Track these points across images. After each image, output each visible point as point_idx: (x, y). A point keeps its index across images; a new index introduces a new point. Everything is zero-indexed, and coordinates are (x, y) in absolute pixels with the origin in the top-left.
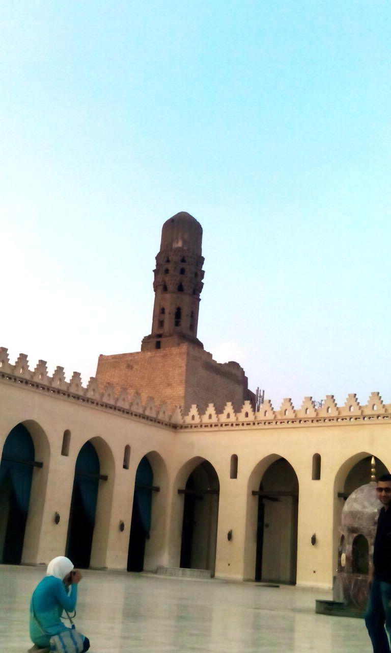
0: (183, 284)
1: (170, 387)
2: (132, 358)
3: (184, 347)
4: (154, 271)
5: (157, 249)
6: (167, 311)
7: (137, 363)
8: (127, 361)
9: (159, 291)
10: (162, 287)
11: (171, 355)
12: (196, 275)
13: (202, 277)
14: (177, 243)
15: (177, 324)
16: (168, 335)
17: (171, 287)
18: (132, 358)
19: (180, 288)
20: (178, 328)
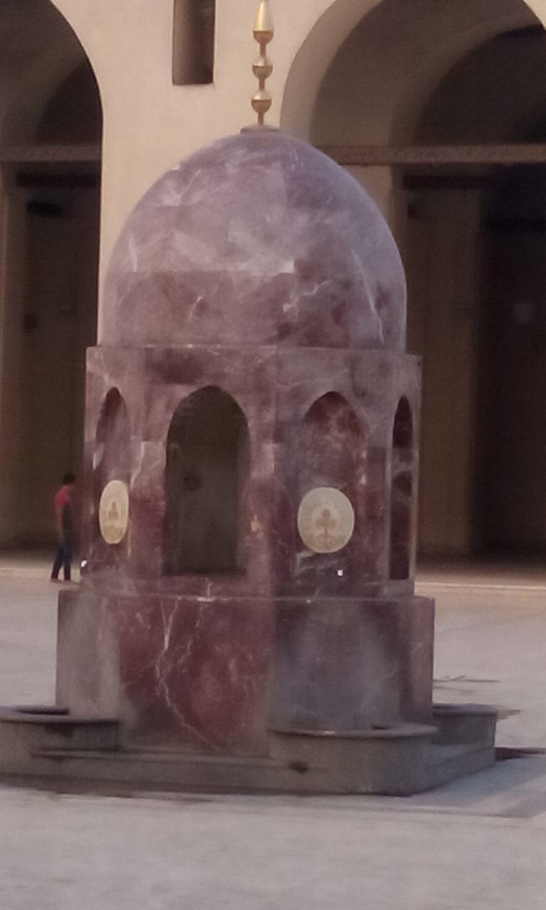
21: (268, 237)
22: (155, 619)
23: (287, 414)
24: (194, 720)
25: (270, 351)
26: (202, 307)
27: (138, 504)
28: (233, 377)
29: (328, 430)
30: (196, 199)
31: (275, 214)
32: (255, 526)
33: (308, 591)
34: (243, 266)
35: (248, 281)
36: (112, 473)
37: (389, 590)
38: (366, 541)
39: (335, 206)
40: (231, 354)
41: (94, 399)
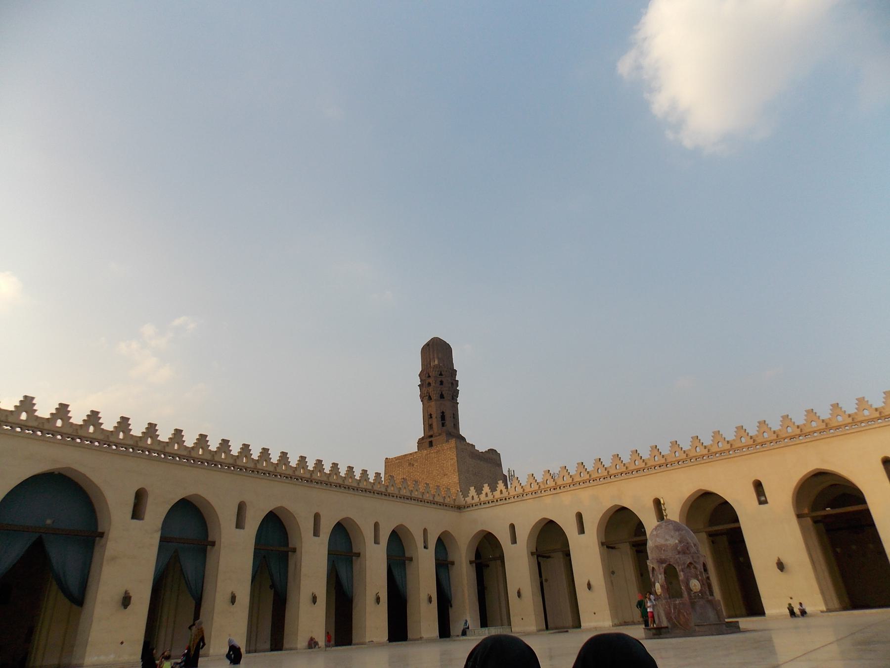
0: (443, 393)
1: (446, 476)
2: (412, 457)
3: (453, 442)
4: (419, 386)
5: (419, 368)
6: (434, 416)
7: (416, 461)
8: (408, 460)
9: (425, 401)
10: (427, 397)
11: (443, 450)
12: (452, 384)
13: (458, 386)
14: (435, 362)
15: (443, 425)
16: (438, 434)
17: (434, 397)
18: (412, 457)
19: (442, 396)
20: (444, 428)
21: (672, 537)
22: (670, 607)
23: (683, 567)
24: (681, 625)
25: (677, 556)
26: (664, 550)
27: (662, 586)
28: (672, 562)
29: (691, 569)
30: (659, 532)
31: (672, 533)
32: (683, 588)
33: (695, 599)
34: (669, 542)
35: (671, 545)
36: (656, 582)
37: (710, 598)
38: (703, 589)
39: (682, 530)
40: (671, 558)
41: (650, 569)
